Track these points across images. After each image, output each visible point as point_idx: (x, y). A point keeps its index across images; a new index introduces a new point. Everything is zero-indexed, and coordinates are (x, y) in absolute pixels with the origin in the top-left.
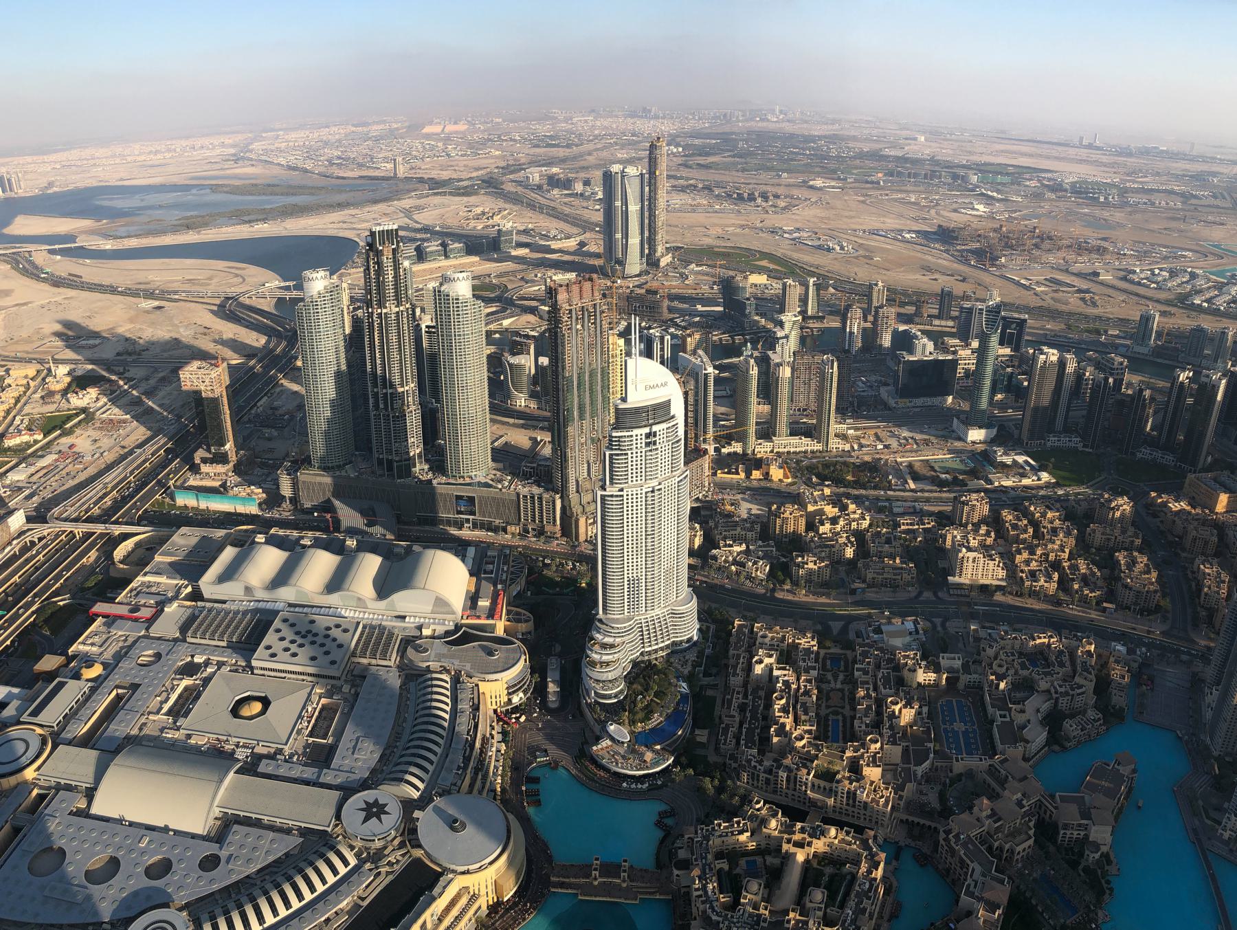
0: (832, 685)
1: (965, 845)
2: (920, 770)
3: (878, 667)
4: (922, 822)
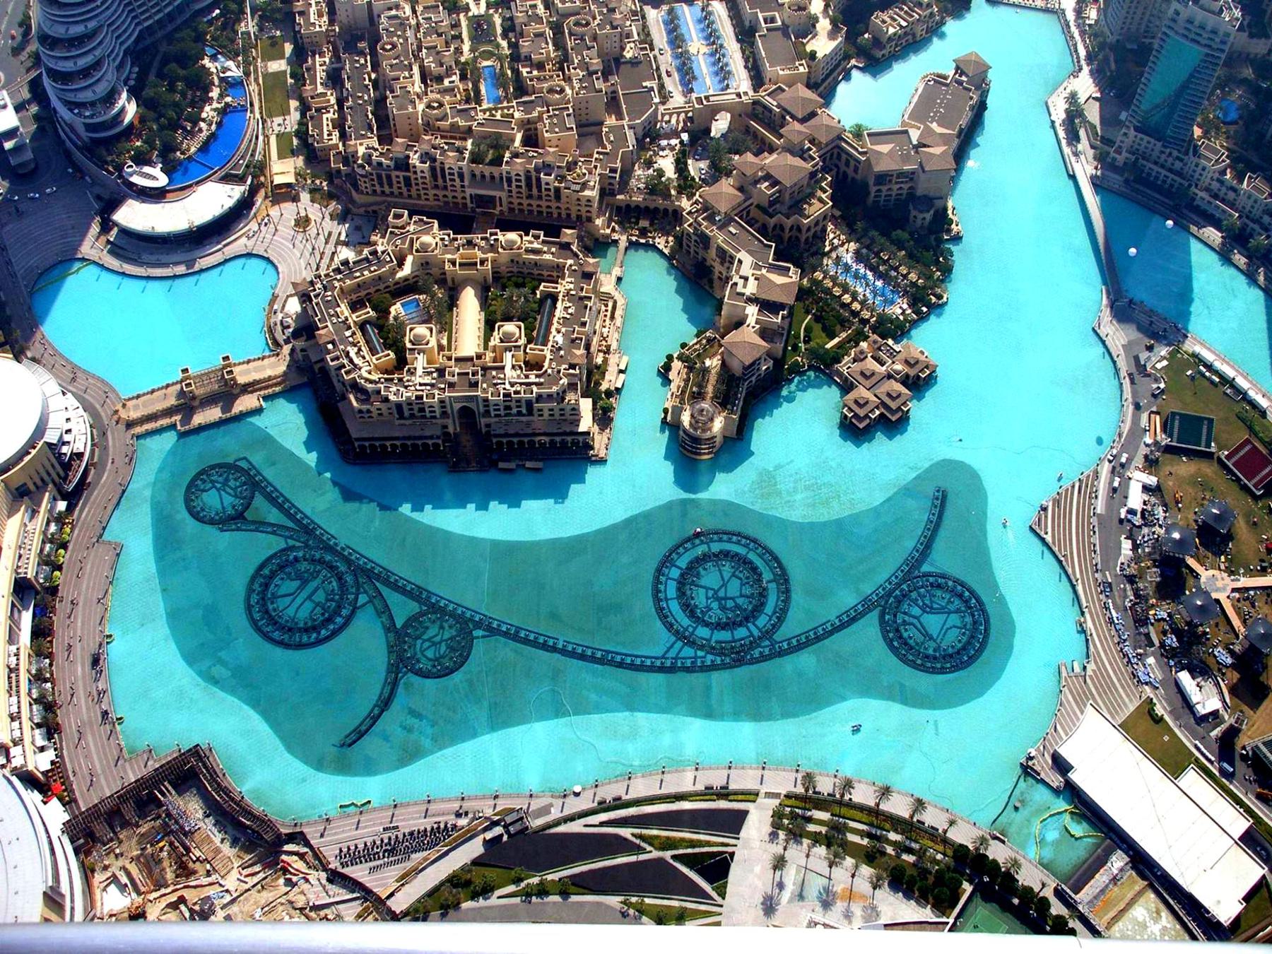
0: (474, 11)
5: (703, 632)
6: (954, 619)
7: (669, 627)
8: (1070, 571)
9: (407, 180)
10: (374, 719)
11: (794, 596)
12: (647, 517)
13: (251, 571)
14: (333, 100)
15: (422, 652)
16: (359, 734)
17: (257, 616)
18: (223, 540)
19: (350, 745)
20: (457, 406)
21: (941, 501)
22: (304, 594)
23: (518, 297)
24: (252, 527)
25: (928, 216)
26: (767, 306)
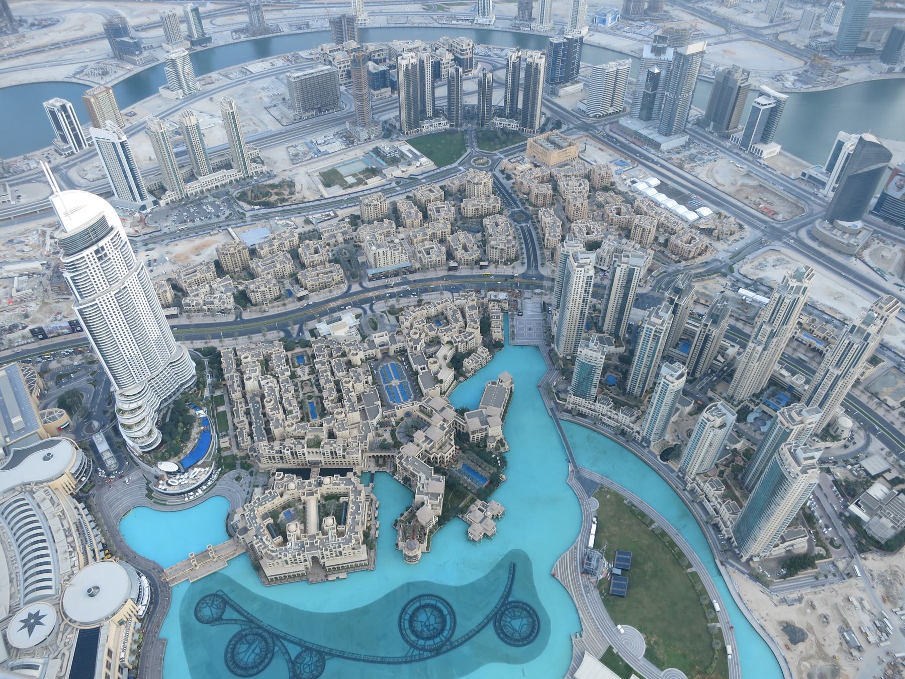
1: (413, 464)
3: (331, 355)
5: (421, 642)
6: (525, 621)
7: (407, 642)
9: (282, 458)
11: (458, 620)
12: (393, 593)
13: (226, 643)
14: (246, 422)
17: (230, 664)
18: (213, 630)
20: (310, 557)
21: (513, 568)
22: (251, 651)
23: (332, 505)
25: (495, 444)
26: (435, 496)
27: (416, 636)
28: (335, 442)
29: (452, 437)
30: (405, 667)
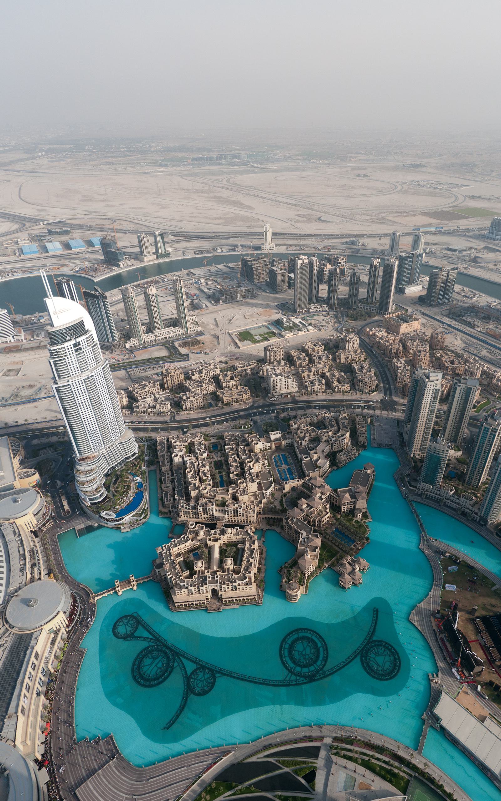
0: (216, 459)
1: (296, 523)
2: (268, 492)
3: (238, 445)
4: (273, 517)
5: (298, 669)
7: (286, 668)
8: (426, 636)
10: (177, 715)
14: (171, 487)
15: (197, 684)
16: (172, 723)
19: (168, 728)
24: (136, 638)
27: (294, 662)
28: (237, 503)
29: (328, 507)
30: (283, 690)
